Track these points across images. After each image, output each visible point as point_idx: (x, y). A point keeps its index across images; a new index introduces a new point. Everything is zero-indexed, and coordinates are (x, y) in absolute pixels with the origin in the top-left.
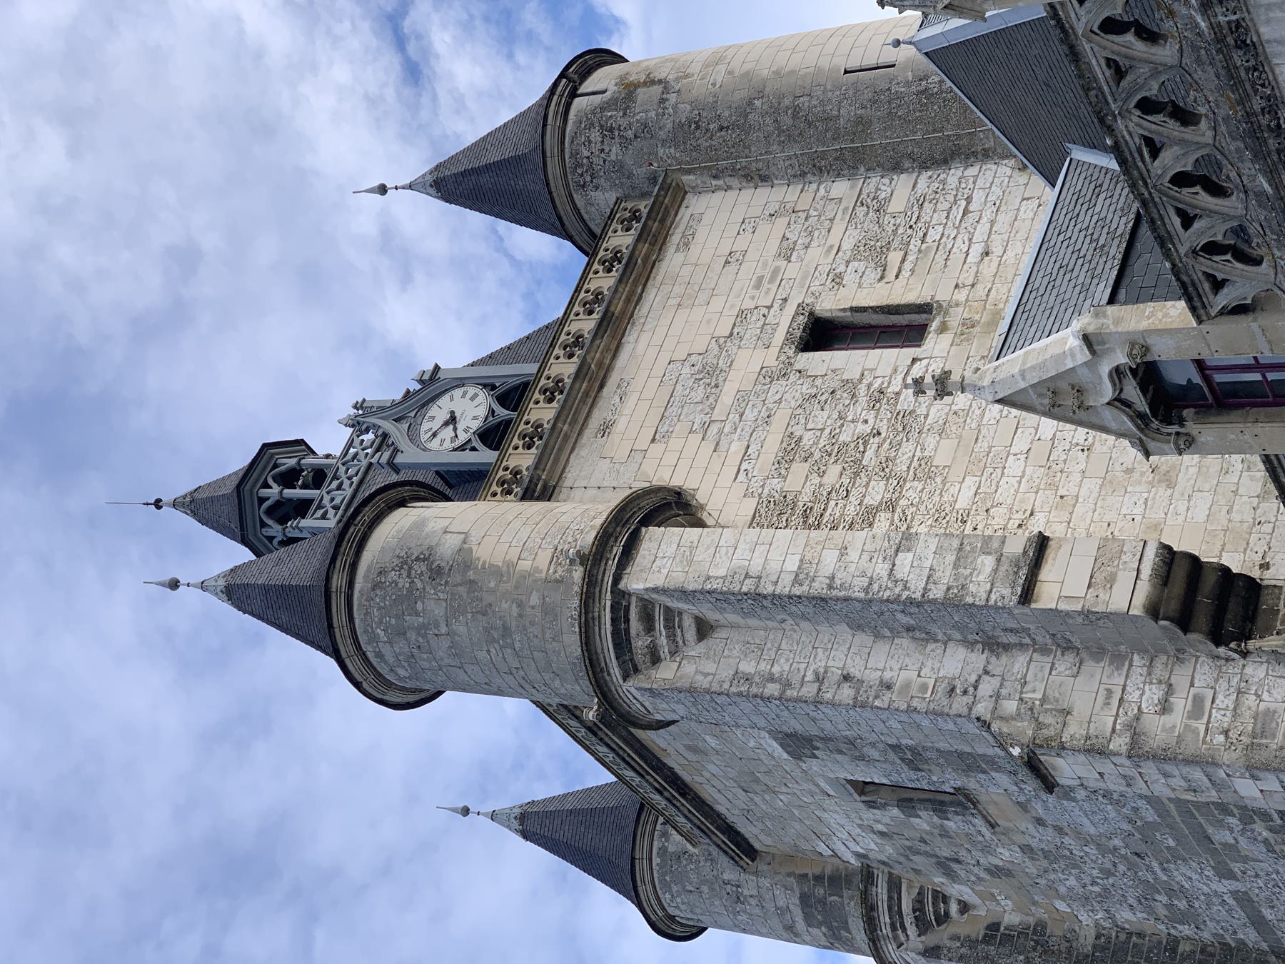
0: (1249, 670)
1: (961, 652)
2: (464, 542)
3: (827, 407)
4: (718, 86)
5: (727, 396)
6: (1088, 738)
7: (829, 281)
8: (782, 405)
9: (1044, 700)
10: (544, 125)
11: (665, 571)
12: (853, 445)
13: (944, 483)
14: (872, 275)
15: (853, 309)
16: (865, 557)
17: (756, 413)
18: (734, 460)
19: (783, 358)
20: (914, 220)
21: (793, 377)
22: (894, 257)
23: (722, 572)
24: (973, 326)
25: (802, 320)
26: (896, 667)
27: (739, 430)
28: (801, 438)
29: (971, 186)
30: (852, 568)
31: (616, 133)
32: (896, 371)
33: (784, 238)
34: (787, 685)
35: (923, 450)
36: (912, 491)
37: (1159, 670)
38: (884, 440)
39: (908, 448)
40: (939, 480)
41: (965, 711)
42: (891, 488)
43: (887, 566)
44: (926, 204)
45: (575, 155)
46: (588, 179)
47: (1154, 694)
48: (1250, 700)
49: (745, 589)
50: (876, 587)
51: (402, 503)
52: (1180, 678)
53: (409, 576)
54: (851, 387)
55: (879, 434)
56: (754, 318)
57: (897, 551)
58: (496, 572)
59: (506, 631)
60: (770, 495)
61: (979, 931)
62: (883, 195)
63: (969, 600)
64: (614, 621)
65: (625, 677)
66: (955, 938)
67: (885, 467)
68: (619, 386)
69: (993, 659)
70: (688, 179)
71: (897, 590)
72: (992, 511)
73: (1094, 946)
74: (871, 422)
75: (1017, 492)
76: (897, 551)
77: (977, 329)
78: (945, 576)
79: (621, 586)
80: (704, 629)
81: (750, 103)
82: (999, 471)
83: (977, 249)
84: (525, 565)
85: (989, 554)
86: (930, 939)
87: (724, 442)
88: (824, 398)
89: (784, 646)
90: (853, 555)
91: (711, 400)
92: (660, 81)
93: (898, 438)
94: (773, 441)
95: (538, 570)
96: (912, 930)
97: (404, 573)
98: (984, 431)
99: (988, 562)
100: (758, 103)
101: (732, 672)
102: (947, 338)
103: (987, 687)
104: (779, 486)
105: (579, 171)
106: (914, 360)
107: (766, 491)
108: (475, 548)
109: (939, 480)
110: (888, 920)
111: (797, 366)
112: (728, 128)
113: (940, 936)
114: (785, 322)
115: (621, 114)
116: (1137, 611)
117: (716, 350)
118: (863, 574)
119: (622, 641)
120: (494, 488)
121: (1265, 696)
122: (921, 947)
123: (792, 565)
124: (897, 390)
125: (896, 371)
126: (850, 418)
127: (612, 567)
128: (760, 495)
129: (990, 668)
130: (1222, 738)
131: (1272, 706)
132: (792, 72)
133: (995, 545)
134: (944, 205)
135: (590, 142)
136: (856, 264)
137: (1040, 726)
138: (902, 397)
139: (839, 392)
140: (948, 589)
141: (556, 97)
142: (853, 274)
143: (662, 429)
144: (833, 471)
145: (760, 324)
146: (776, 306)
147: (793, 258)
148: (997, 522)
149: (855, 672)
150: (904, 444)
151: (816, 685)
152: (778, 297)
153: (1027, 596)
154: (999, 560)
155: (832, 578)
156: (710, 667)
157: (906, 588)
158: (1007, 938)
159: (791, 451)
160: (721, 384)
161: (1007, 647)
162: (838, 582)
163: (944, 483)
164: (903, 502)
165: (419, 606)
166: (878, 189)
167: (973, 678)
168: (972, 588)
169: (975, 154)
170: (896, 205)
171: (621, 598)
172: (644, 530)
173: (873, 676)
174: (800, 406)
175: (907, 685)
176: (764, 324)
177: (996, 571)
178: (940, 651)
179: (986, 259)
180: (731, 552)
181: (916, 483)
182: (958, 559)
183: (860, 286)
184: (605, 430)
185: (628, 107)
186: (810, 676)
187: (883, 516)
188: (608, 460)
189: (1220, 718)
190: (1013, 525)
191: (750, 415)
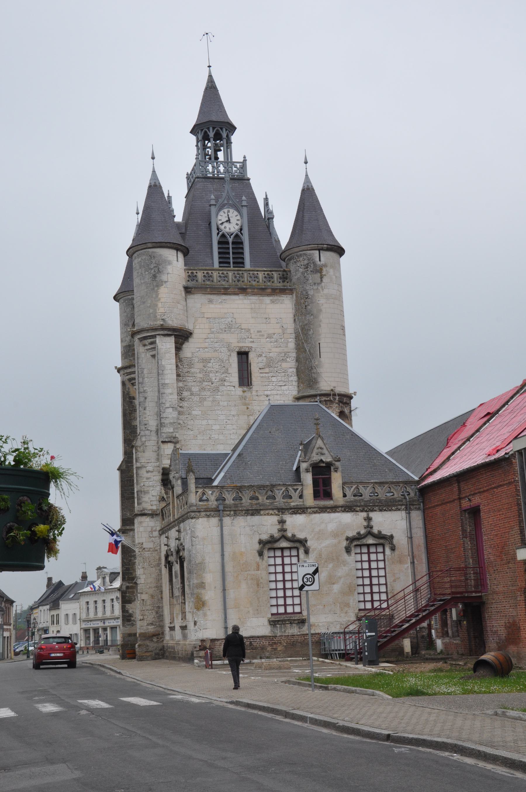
0: (158, 487)
1: (155, 424)
2: (165, 282)
3: (220, 367)
4: (318, 302)
5: (221, 336)
6: (139, 458)
7: (259, 353)
8: (220, 354)
9: (146, 446)
10: (307, 245)
11: (162, 347)
12: (209, 378)
13: (199, 406)
14: (261, 365)
15: (250, 363)
16: (170, 400)
17: (217, 346)
18: (203, 345)
19: (235, 348)
20: (279, 372)
21: (228, 353)
22: (267, 370)
23: (163, 363)
24: (245, 399)
25: (247, 350)
26: (150, 410)
27: (211, 343)
28: (209, 362)
29: (289, 384)
30: (167, 398)
31: (306, 270)
32: (231, 382)
33: (274, 334)
34: (142, 383)
35: (208, 397)
36: (196, 398)
37: (156, 469)
38: (211, 386)
39: (209, 393)
40: (200, 404)
41: (141, 429)
42: (197, 393)
43: (168, 406)
44: (284, 373)
45: (301, 255)
46: (295, 261)
47: (150, 468)
48: (152, 489)
49: (159, 371)
50: (163, 405)
51: (177, 250)
52: (155, 473)
53: (154, 267)
54: (226, 372)
55: (212, 384)
56: (247, 334)
57: (173, 407)
58: (157, 296)
59: (144, 303)
60: (193, 360)
61: (132, 394)
62: (288, 359)
63: (162, 429)
64: (149, 336)
65: (139, 339)
66: (129, 388)
67: (203, 389)
68: (224, 300)
69: (154, 432)
70: (294, 295)
71: (163, 411)
72: (192, 421)
73: (134, 426)
74: (216, 381)
75: (198, 425)
76: (173, 407)
77: (244, 401)
78: (167, 421)
79: (157, 336)
80: (153, 356)
81: (312, 315)
82: (203, 419)
83: (268, 393)
84: (160, 305)
85: (174, 430)
86: (127, 383)
87: (207, 340)
88: (223, 365)
89: (152, 379)
90: (171, 397)
91: (221, 331)
92: (322, 281)
93: (211, 390)
94: (207, 355)
95: (159, 309)
96: (128, 377)
97: (155, 265)
98: (214, 412)
99: (171, 430)
100: (312, 317)
101: (144, 368)
102: (241, 393)
103: (147, 432)
104: (195, 361)
105: (297, 257)
106: (234, 387)
107: (194, 358)
108: (163, 286)
109: (200, 404)
110: (128, 372)
111: (232, 354)
112: (306, 308)
113: (128, 385)
114: (245, 345)
115: (312, 270)
116: (163, 466)
117: (237, 326)
118: (166, 401)
119: (145, 338)
120: (190, 272)
121: (153, 491)
122: (125, 380)
123: (167, 381)
124: (225, 385)
125: (231, 382)
126: (217, 374)
127: (162, 332)
128: (193, 357)
129: (152, 432)
130: (142, 485)
131: (151, 493)
132: (320, 326)
133: (176, 431)
134: (283, 379)
135: (304, 261)
136: (265, 359)
137: (140, 447)
138: (223, 387)
139: (224, 369)
140: (164, 423)
141: (316, 246)
142: (261, 360)
143: (211, 320)
144: (201, 375)
145: (245, 337)
146: (251, 340)
147: (268, 339)
148: (189, 423)
149: (147, 399)
150: (209, 392)
151: (143, 391)
152: (254, 339)
153: (163, 442)
154: (172, 433)
155: (164, 393)
156: (144, 361)
157: (163, 413)
158: (131, 402)
159: (205, 361)
160: (226, 332)
161: (157, 434)
162: (163, 395)
163: (199, 406)
164: (193, 397)
165: (147, 273)
166: (290, 357)
167: (149, 429)
168: (165, 428)
169: (298, 384)
170: (284, 365)
171: (154, 336)
172: (173, 336)
173: (147, 405)
174: (220, 359)
175: (145, 414)
176: (245, 338)
177: (169, 433)
178: (155, 419)
179: (265, 397)
180: (169, 363)
181: (198, 399)
182: (171, 423)
183: (257, 363)
184: (211, 301)
185: (313, 272)
186: (145, 388)
187: (189, 393)
188: (200, 306)
189: (147, 484)
190: (189, 427)
191: (216, 345)
